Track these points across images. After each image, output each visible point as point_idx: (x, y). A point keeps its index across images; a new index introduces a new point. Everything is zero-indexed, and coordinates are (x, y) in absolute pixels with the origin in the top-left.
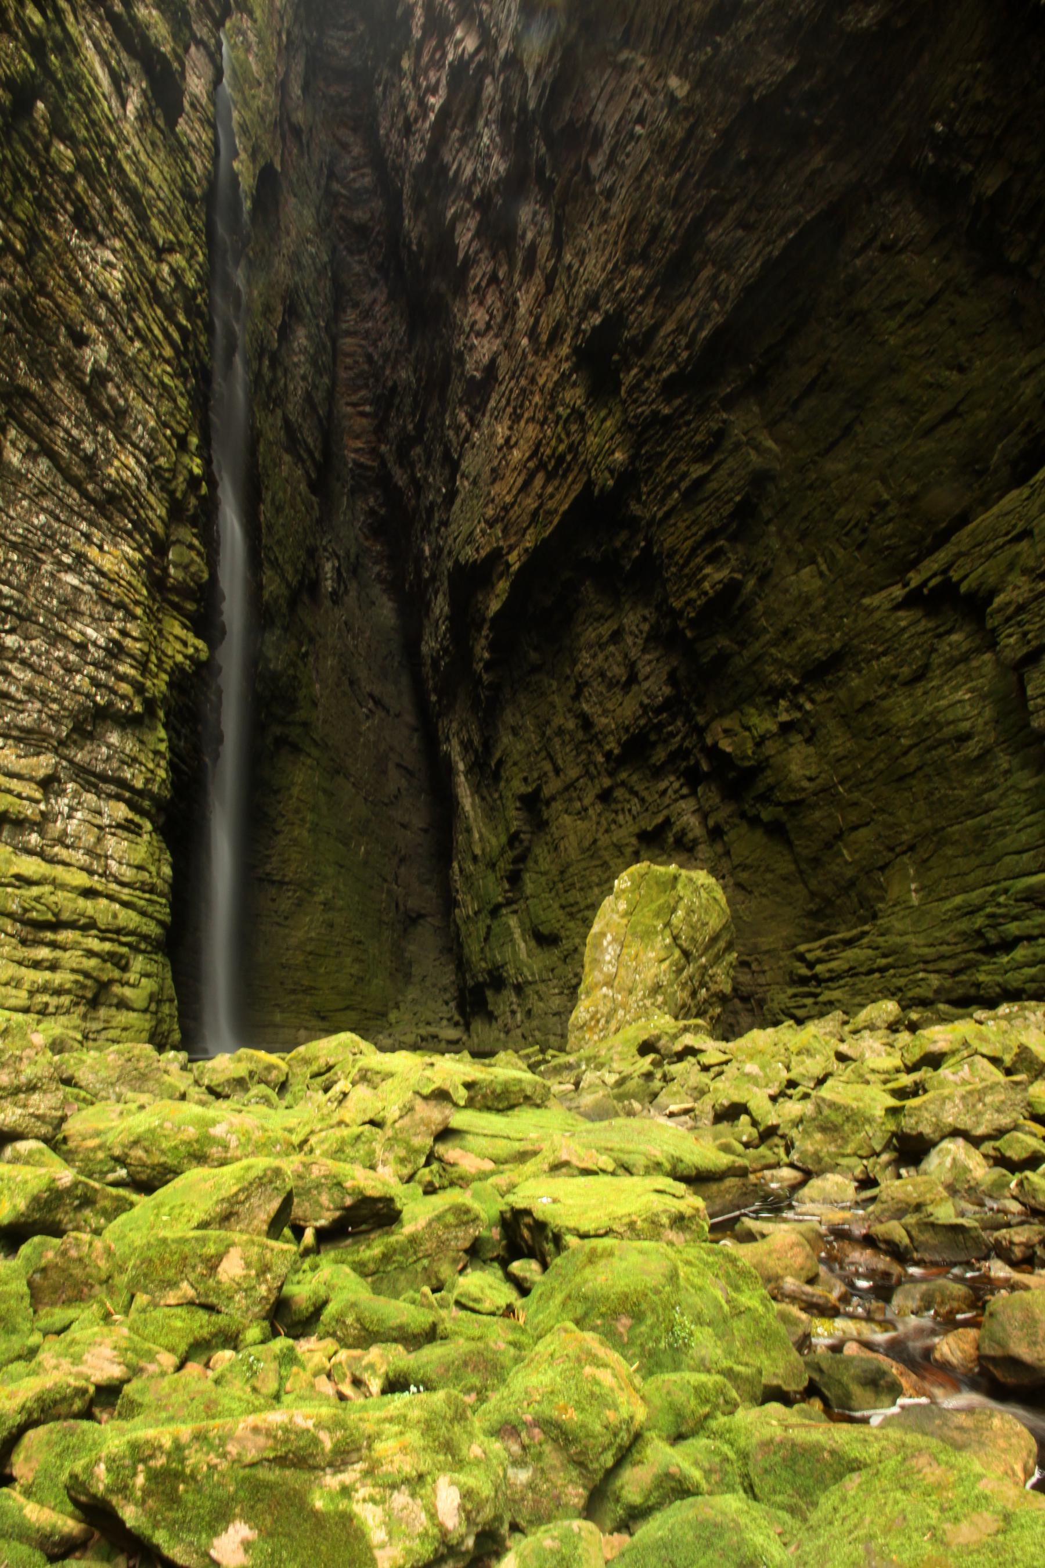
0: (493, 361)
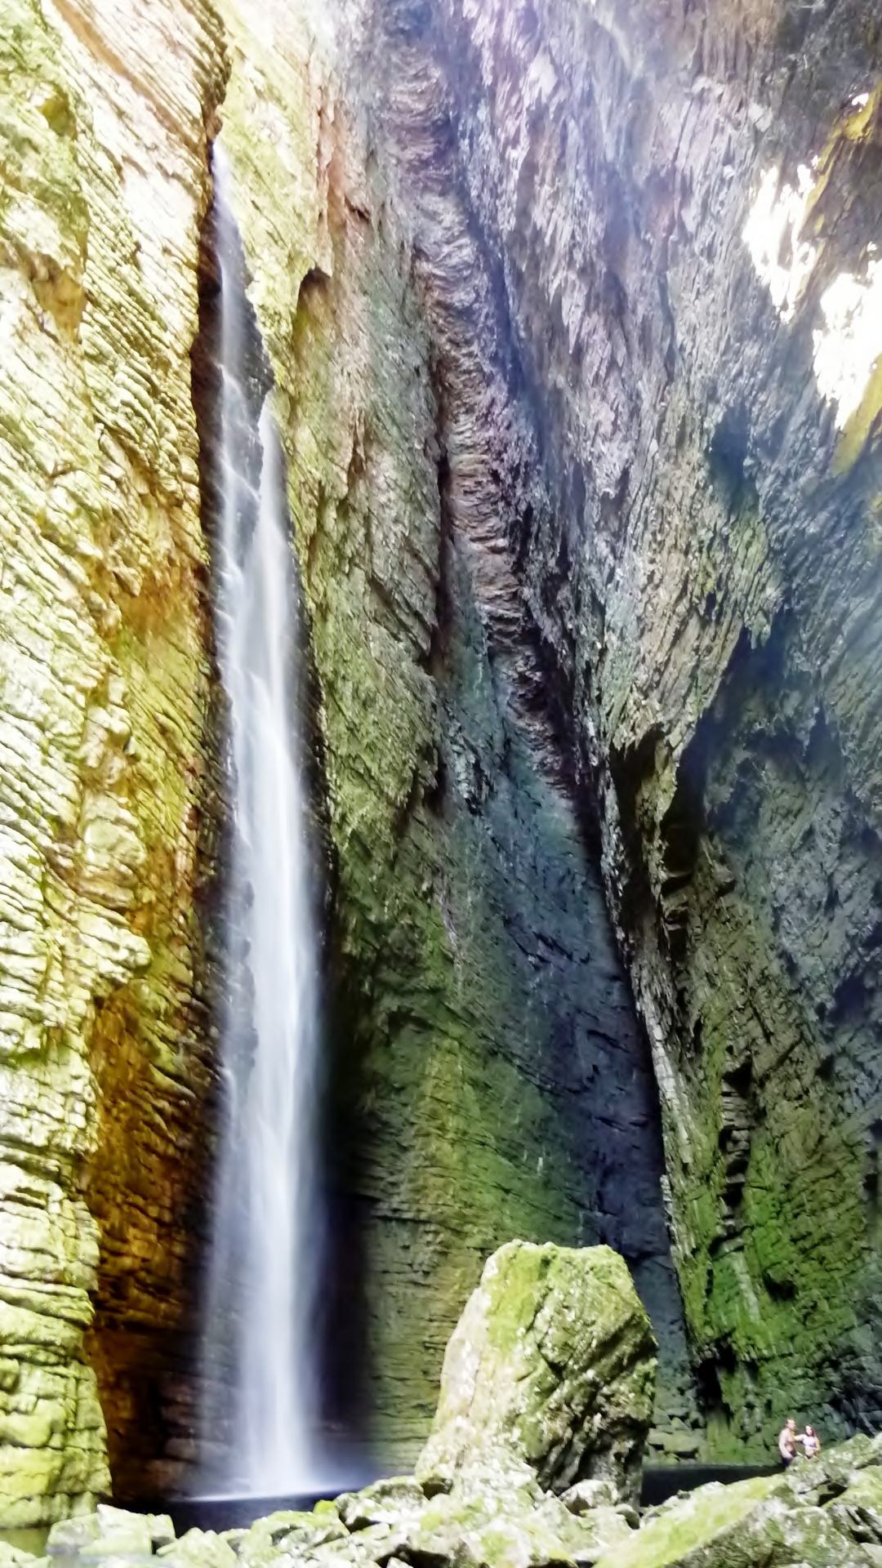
0: (625, 473)
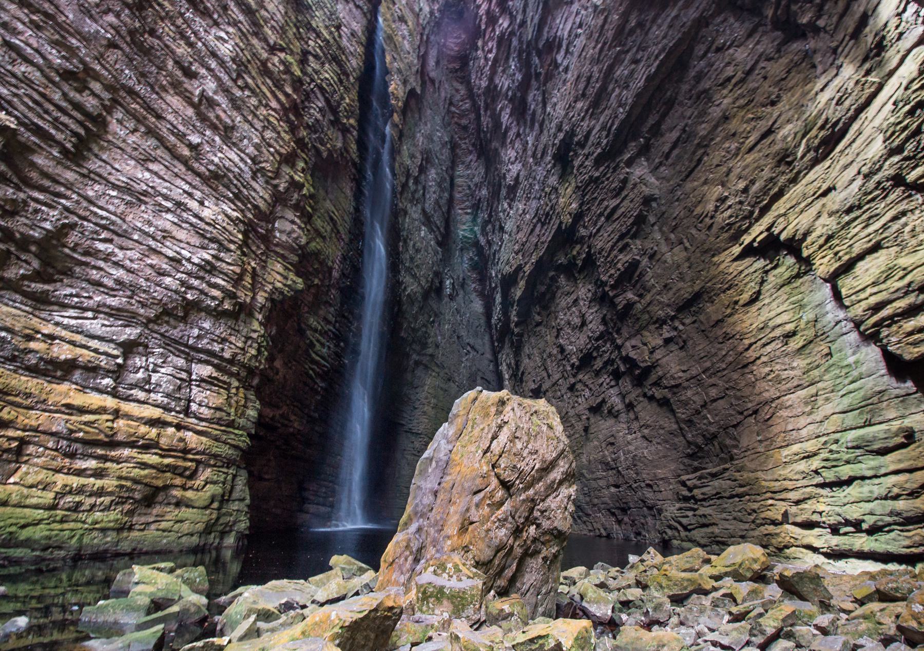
0: (518, 175)
